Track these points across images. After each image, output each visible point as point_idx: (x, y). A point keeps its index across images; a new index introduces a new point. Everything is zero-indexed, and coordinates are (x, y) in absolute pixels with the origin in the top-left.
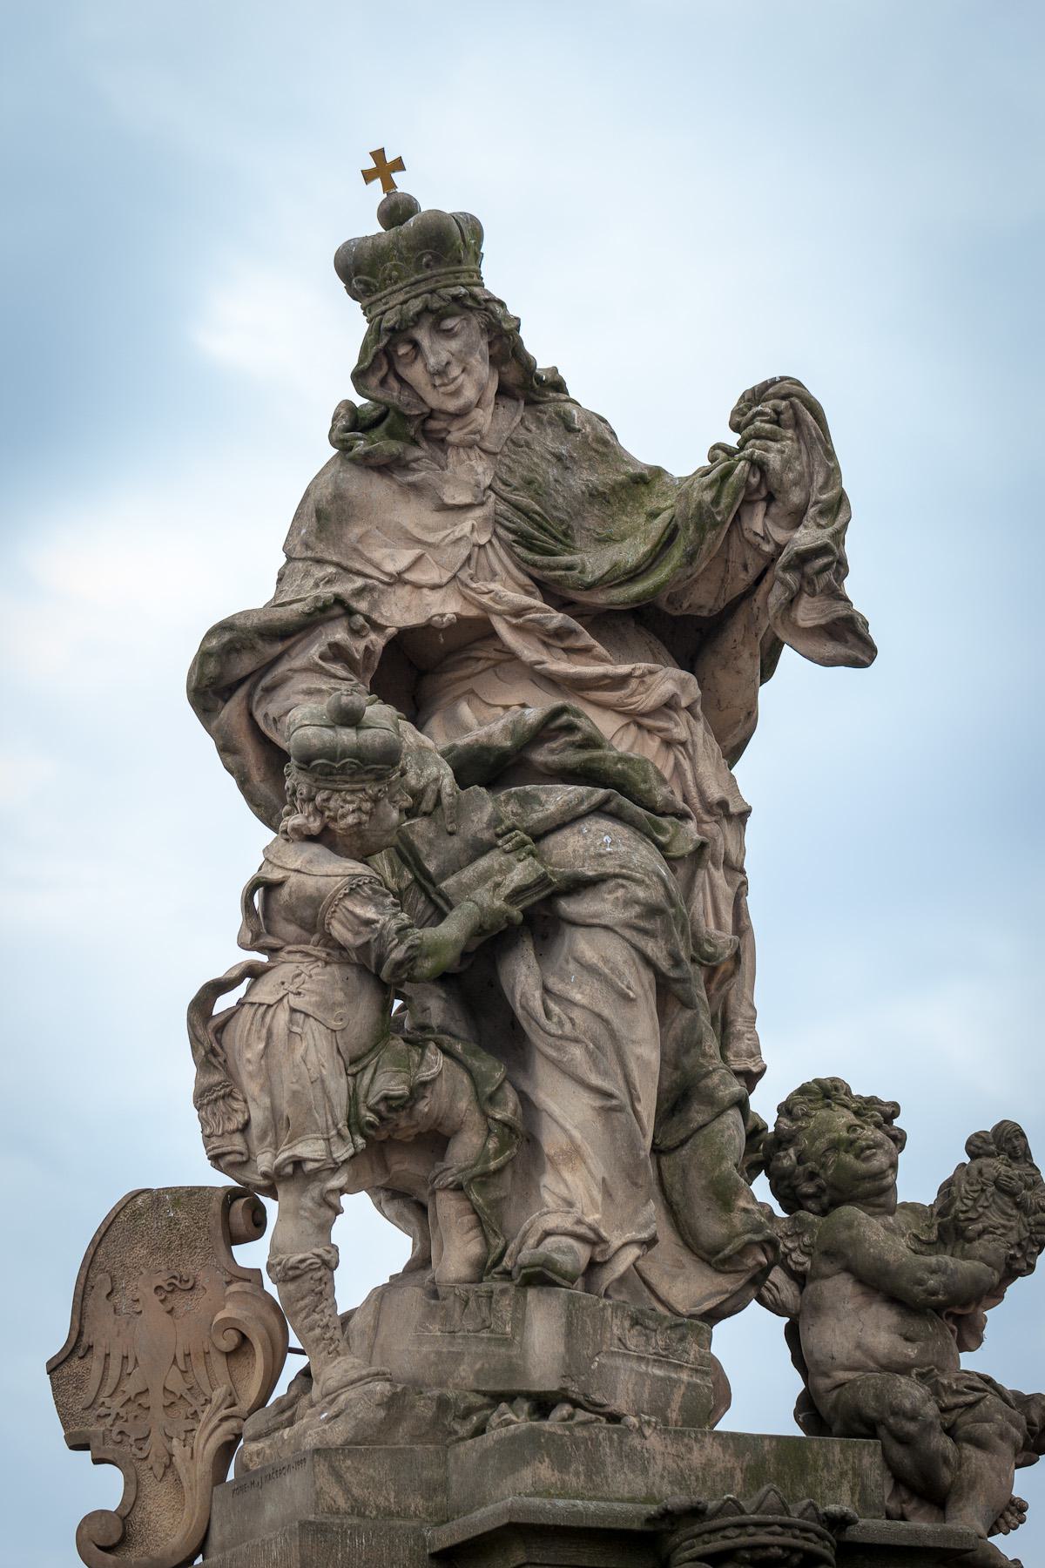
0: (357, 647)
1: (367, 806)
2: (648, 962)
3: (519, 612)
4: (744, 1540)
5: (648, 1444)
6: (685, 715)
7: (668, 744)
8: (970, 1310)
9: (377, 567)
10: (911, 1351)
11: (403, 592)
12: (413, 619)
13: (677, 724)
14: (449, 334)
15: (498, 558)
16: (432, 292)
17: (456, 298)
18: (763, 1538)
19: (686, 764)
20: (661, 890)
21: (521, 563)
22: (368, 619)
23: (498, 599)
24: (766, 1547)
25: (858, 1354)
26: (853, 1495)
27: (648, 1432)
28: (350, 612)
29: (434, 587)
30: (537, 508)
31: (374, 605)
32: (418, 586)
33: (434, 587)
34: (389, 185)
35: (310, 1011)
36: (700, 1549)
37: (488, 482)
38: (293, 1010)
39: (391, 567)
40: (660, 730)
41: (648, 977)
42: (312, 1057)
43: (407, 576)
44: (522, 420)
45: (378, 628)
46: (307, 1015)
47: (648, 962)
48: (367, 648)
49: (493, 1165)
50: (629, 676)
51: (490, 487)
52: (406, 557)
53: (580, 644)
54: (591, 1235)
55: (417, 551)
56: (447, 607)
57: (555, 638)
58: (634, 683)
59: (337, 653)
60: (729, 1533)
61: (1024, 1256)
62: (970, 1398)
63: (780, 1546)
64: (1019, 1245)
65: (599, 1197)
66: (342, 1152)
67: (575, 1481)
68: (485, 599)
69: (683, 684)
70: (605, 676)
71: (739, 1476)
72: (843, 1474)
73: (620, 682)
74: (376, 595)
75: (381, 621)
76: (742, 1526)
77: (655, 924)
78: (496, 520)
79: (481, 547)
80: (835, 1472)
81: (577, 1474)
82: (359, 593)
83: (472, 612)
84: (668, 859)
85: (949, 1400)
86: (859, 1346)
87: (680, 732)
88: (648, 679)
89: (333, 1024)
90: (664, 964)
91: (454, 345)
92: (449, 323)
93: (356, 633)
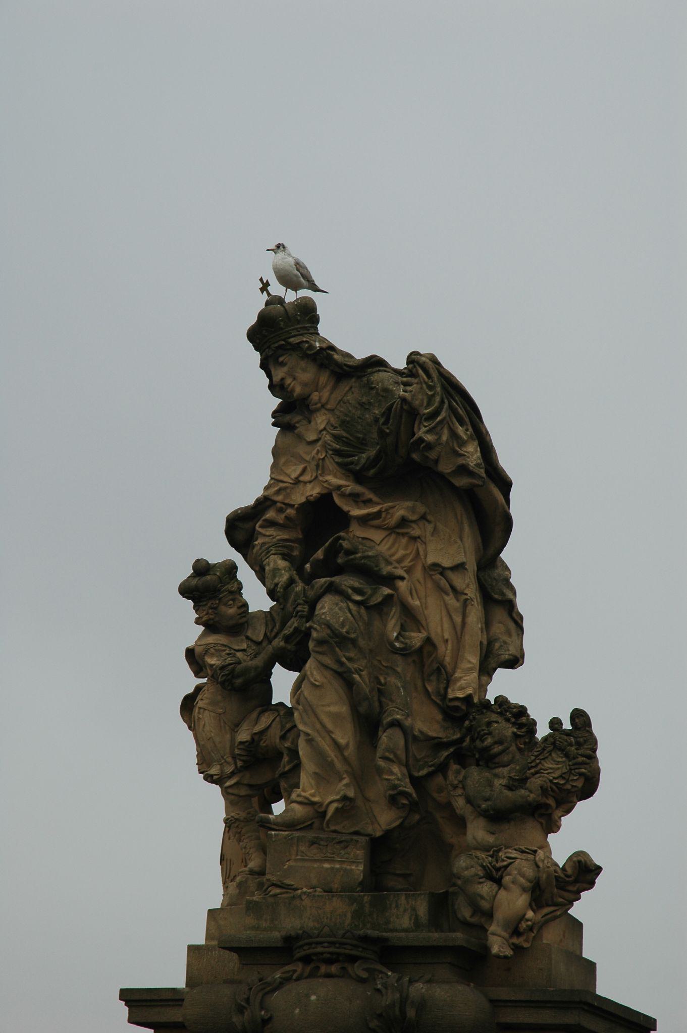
0: (280, 518)
1: (210, 611)
2: (326, 667)
3: (339, 487)
4: (311, 951)
5: (304, 903)
6: (421, 523)
7: (415, 539)
8: (550, 811)
9: (289, 476)
10: (491, 839)
11: (301, 486)
12: (303, 500)
13: (414, 529)
14: (282, 364)
15: (330, 464)
16: (269, 347)
17: (280, 347)
18: (319, 949)
19: (421, 550)
20: (329, 631)
21: (339, 464)
22: (284, 504)
23: (329, 484)
24: (322, 954)
25: (474, 842)
26: (410, 919)
27: (304, 897)
28: (275, 502)
29: (310, 482)
30: (344, 434)
31: (288, 496)
32: (305, 483)
33: (310, 482)
34: (269, 294)
35: (205, 707)
36: (298, 955)
37: (322, 427)
38: (200, 708)
39: (294, 476)
40: (407, 533)
41: (328, 674)
42: (207, 728)
43: (301, 479)
44: (351, 388)
45: (292, 506)
46: (205, 709)
47: (326, 667)
48: (286, 517)
49: (287, 768)
50: (380, 512)
51: (325, 429)
52: (300, 468)
53: (365, 498)
54: (306, 801)
55: (302, 466)
56: (313, 491)
57: (355, 498)
58: (383, 515)
59: (271, 524)
60: (305, 948)
61: (568, 781)
62: (505, 863)
63: (330, 953)
64: (564, 778)
65: (313, 782)
66: (229, 769)
67: (264, 924)
68: (325, 485)
69: (413, 510)
70: (368, 515)
71: (349, 915)
72: (405, 911)
73: (378, 515)
74: (288, 491)
75: (292, 503)
76: (310, 944)
77: (324, 648)
78: (325, 446)
79: (323, 459)
80: (401, 909)
81: (266, 920)
82: (278, 492)
83: (325, 491)
84: (368, 608)
85: (499, 864)
86: (474, 838)
87: (416, 532)
88: (391, 511)
89: (220, 711)
90: (335, 667)
91: (285, 369)
92: (281, 359)
93: (281, 511)
